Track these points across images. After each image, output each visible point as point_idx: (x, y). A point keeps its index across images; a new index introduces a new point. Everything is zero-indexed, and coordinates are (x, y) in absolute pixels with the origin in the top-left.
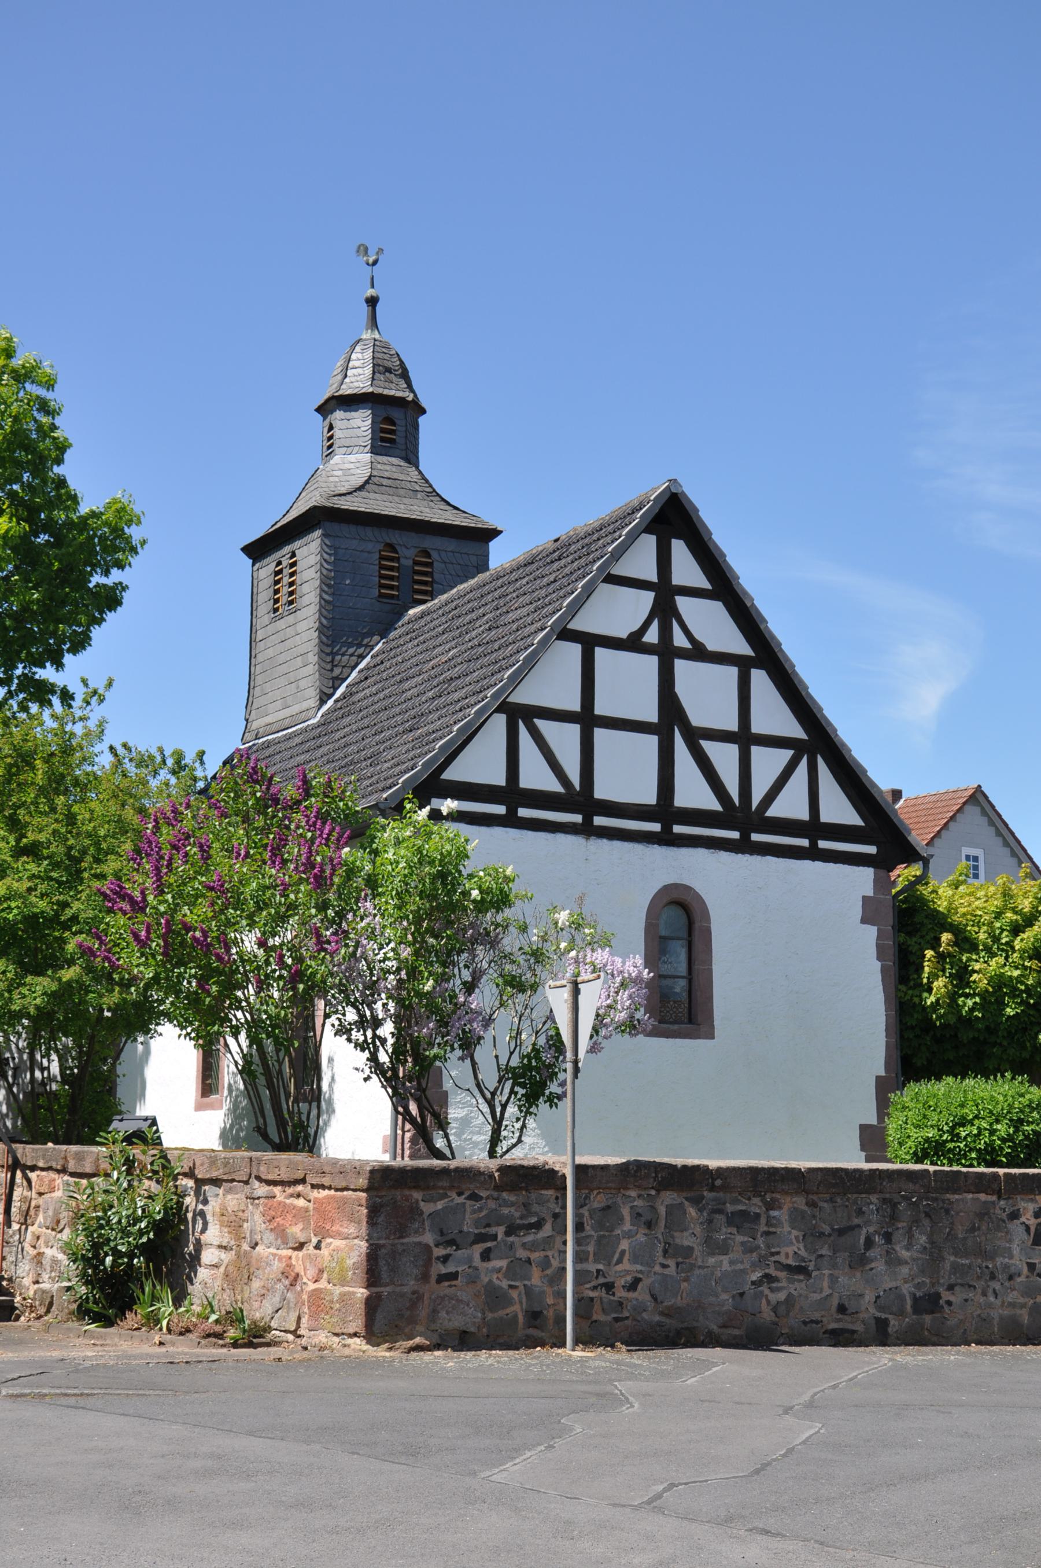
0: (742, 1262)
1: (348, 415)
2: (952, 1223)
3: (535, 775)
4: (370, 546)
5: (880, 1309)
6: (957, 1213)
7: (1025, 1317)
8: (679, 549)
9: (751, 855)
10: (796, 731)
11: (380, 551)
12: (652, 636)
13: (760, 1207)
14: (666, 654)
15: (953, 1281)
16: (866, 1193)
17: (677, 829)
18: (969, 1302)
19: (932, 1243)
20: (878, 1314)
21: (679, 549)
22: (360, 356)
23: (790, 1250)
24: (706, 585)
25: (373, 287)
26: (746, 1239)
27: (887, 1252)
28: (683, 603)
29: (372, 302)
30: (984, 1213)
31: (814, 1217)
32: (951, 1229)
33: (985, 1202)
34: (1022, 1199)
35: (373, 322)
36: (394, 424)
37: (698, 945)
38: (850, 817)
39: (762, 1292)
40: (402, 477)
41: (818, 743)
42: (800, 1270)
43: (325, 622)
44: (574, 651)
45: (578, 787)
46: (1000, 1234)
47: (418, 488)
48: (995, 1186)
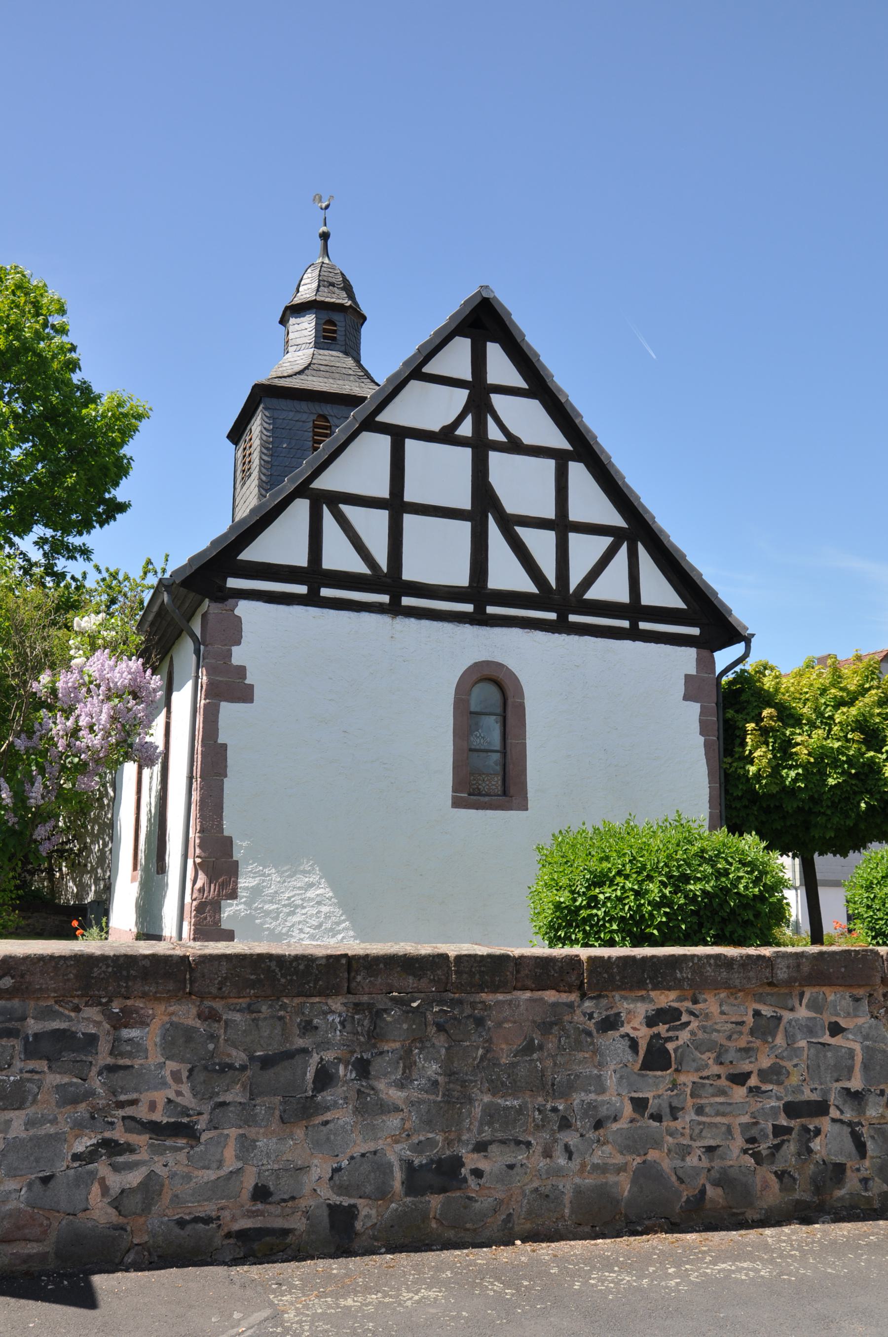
0: (54, 1121)
1: (298, 320)
2: (489, 1041)
3: (339, 556)
4: (304, 417)
5: (342, 1189)
6: (499, 1025)
7: (624, 1186)
8: (494, 352)
9: (568, 634)
10: (616, 519)
11: (314, 421)
12: (466, 429)
13: (98, 1024)
14: (480, 447)
15: (487, 1135)
16: (320, 995)
17: (491, 610)
18: (518, 1169)
19: (450, 1074)
20: (336, 1199)
21: (494, 352)
22: (310, 275)
23: (160, 1096)
24: (522, 384)
25: (325, 225)
26: (66, 1080)
27: (359, 1092)
28: (498, 401)
29: (325, 236)
30: (551, 1022)
31: (212, 1037)
32: (487, 1051)
33: (555, 1005)
34: (626, 998)
35: (326, 252)
36: (335, 325)
37: (511, 721)
38: (672, 600)
39: (93, 1174)
40: (338, 364)
41: (638, 530)
42: (181, 1130)
43: (264, 478)
44: (384, 442)
45: (385, 569)
46: (580, 1055)
47: (351, 372)
48: (573, 978)
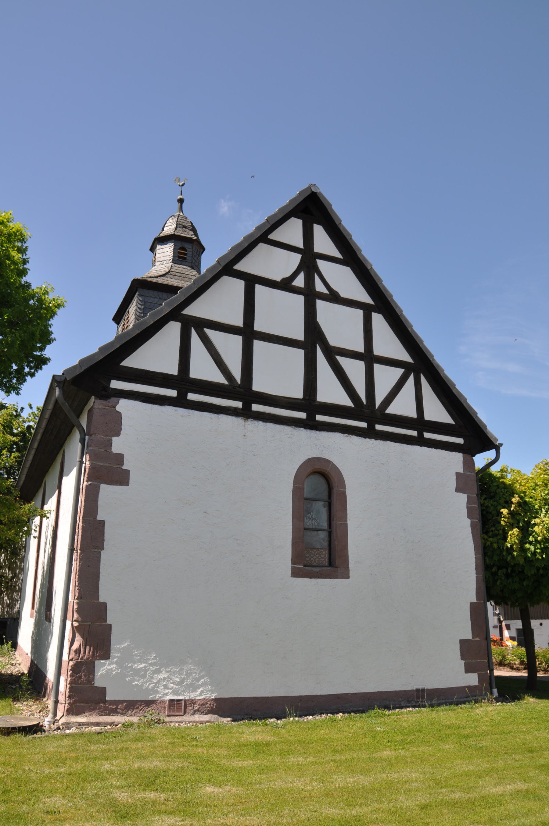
1: (163, 247)
3: (202, 368)
8: (319, 231)
9: (376, 439)
10: (405, 356)
12: (300, 282)
14: (310, 297)
17: (319, 418)
21: (319, 231)
22: (171, 221)
24: (339, 255)
28: (322, 264)
29: (181, 201)
36: (186, 250)
41: (421, 365)
44: (240, 285)
45: (239, 381)
